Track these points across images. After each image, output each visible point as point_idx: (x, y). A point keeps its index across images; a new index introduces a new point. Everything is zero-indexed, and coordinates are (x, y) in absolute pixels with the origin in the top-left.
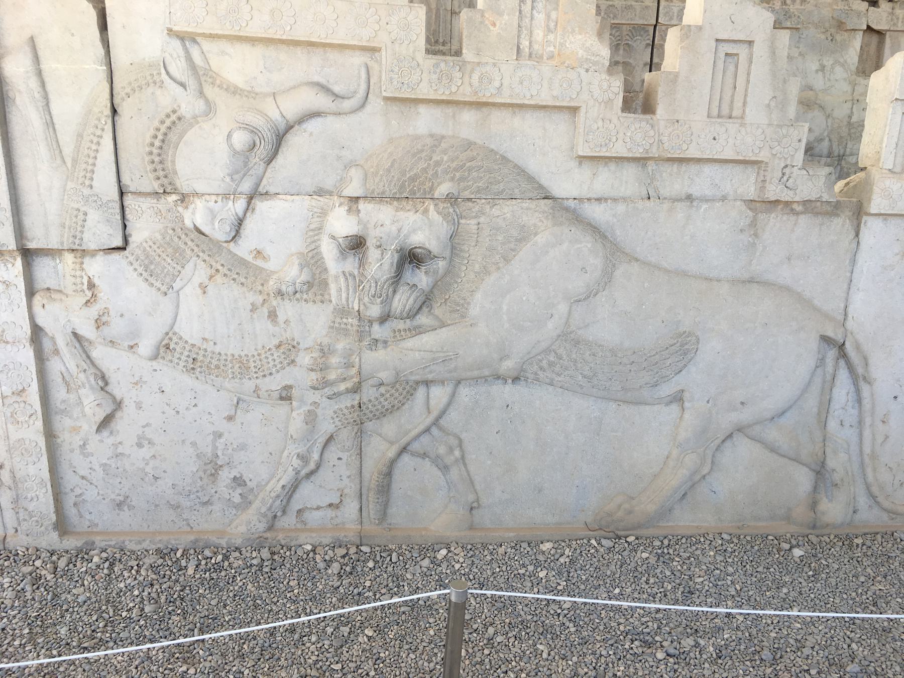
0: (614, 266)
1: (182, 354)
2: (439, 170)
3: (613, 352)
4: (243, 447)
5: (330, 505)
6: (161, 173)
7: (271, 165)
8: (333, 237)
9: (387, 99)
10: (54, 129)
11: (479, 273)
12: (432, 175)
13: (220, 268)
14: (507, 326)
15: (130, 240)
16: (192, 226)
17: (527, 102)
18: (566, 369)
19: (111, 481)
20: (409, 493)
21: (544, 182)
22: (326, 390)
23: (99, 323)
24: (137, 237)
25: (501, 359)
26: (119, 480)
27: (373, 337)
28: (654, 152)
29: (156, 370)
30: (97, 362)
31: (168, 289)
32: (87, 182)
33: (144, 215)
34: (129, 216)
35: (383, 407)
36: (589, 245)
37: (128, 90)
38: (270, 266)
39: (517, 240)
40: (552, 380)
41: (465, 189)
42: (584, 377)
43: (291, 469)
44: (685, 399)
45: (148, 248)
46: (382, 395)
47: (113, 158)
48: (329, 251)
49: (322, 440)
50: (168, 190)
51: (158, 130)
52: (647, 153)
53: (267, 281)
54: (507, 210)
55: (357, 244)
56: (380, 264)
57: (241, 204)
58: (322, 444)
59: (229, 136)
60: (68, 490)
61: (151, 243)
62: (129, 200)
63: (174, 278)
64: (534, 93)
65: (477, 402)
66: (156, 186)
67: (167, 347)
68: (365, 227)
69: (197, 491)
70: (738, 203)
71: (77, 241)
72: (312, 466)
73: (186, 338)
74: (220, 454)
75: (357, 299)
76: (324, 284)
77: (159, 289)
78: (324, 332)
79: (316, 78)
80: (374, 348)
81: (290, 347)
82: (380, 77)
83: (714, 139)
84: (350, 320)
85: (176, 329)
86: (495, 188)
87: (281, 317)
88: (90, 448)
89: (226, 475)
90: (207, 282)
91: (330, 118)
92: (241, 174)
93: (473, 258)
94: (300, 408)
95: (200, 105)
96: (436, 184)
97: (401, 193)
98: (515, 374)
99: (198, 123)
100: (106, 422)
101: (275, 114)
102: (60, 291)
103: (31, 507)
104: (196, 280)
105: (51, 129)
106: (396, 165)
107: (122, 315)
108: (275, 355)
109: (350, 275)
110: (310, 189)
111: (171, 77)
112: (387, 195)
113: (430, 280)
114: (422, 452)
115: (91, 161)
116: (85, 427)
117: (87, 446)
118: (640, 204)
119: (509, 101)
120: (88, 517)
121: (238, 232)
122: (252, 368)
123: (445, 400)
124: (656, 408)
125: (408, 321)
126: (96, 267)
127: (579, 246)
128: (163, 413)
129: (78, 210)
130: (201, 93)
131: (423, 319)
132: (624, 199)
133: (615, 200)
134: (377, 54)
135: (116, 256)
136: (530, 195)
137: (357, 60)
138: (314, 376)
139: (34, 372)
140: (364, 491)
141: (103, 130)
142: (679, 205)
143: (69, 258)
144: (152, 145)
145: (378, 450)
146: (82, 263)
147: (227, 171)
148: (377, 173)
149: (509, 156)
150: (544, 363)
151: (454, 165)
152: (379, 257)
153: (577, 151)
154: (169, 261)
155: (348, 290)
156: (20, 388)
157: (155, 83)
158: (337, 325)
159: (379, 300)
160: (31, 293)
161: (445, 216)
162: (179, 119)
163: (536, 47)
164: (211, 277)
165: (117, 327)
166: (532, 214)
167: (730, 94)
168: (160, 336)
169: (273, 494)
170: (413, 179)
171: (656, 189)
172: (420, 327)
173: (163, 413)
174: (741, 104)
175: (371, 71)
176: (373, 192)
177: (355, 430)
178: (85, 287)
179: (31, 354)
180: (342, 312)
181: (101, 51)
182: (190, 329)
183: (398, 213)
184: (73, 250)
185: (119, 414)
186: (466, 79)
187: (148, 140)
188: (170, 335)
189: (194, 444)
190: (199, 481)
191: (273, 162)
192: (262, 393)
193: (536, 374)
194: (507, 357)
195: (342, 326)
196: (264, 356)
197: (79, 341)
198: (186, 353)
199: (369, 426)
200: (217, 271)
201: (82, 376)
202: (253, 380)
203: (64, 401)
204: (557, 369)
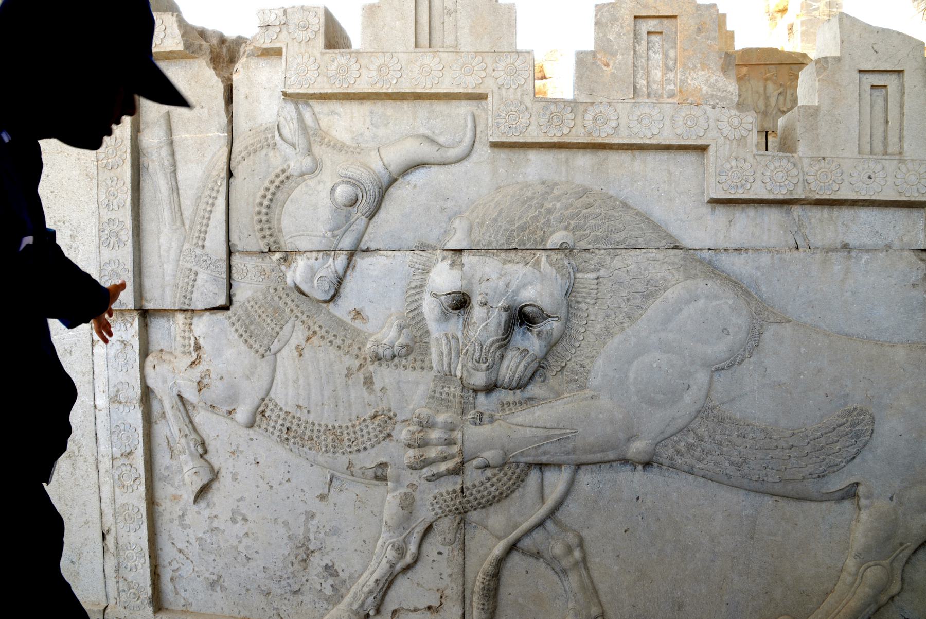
0: (761, 326)
1: (276, 422)
2: (552, 217)
3: (768, 434)
4: (335, 531)
5: (429, 608)
6: (268, 233)
7: (374, 220)
8: (435, 295)
9: (495, 145)
11: (600, 335)
12: (544, 223)
13: (317, 329)
14: (634, 398)
15: (234, 299)
16: (292, 285)
17: (647, 142)
18: (709, 453)
19: (206, 557)
20: (520, 600)
21: (674, 230)
22: (424, 470)
23: (201, 386)
24: (242, 294)
25: (629, 440)
26: (213, 557)
27: (478, 409)
28: (799, 194)
29: (252, 439)
30: (199, 428)
31: (266, 351)
32: (200, 243)
33: (249, 275)
34: (235, 275)
35: (489, 493)
36: (730, 302)
37: (244, 154)
38: (369, 327)
40: (692, 467)
41: (581, 239)
42: (732, 464)
43: (385, 560)
44: (860, 494)
46: (489, 479)
47: (224, 218)
49: (420, 530)
50: (273, 249)
51: (267, 189)
52: (791, 194)
53: (364, 344)
54: (631, 260)
55: (461, 303)
57: (341, 260)
58: (420, 534)
59: (333, 190)
60: (166, 563)
61: (252, 303)
62: (236, 259)
63: (273, 338)
64: (656, 131)
65: (600, 492)
67: (263, 412)
68: (470, 283)
69: (288, 578)
70: (906, 253)
72: (408, 559)
73: (281, 404)
74: (312, 537)
77: (257, 351)
79: (422, 131)
81: (386, 418)
83: (870, 177)
84: (452, 389)
85: (272, 394)
86: (616, 237)
87: (377, 386)
88: (187, 521)
89: (317, 562)
91: (435, 169)
92: (342, 230)
93: (592, 318)
94: (395, 490)
95: (307, 162)
97: (510, 244)
99: (305, 180)
100: (203, 492)
101: (377, 165)
102: (171, 353)
103: (130, 576)
104: (294, 342)
105: (175, 194)
106: (504, 214)
107: (221, 378)
108: (371, 427)
109: (453, 337)
110: (413, 244)
111: (283, 139)
112: (494, 245)
113: (543, 343)
114: (535, 551)
115: (205, 222)
116: (185, 496)
117: (186, 517)
118: (788, 256)
119: (627, 141)
120: (183, 594)
122: (346, 441)
124: (824, 505)
125: (518, 391)
126: (202, 326)
127: (718, 302)
128: (257, 486)
129: (190, 270)
130: (309, 151)
131: (534, 390)
132: (769, 249)
133: (757, 250)
134: (484, 102)
135: (220, 315)
136: (657, 245)
137: (463, 109)
138: (411, 452)
139: (141, 435)
140: (467, 593)
141: (218, 191)
142: (834, 256)
143: (180, 317)
144: (261, 204)
146: (191, 324)
147: (328, 227)
149: (630, 202)
151: (568, 212)
152: (485, 315)
153: (708, 194)
155: (450, 353)
156: (128, 450)
159: (484, 366)
160: (145, 353)
161: (560, 269)
162: (288, 178)
163: (655, 86)
164: (308, 339)
165: (217, 389)
167: (881, 130)
168: (257, 401)
169: (366, 589)
170: (523, 229)
171: (805, 237)
172: (531, 399)
173: (257, 486)
174: (896, 139)
175: (477, 120)
177: (458, 521)
178: (192, 348)
179: (139, 415)
181: (224, 119)
182: (285, 396)
183: (506, 266)
184: (184, 310)
185: (216, 485)
186: (579, 120)
187: (258, 200)
188: (266, 401)
189: (286, 524)
190: (290, 565)
191: (376, 217)
192: (355, 470)
193: (672, 459)
195: (444, 396)
196: (358, 428)
197: (184, 405)
198: (281, 422)
199: (474, 516)
200: (315, 333)
201: (183, 441)
202: (346, 455)
203: (167, 467)
204: (698, 453)
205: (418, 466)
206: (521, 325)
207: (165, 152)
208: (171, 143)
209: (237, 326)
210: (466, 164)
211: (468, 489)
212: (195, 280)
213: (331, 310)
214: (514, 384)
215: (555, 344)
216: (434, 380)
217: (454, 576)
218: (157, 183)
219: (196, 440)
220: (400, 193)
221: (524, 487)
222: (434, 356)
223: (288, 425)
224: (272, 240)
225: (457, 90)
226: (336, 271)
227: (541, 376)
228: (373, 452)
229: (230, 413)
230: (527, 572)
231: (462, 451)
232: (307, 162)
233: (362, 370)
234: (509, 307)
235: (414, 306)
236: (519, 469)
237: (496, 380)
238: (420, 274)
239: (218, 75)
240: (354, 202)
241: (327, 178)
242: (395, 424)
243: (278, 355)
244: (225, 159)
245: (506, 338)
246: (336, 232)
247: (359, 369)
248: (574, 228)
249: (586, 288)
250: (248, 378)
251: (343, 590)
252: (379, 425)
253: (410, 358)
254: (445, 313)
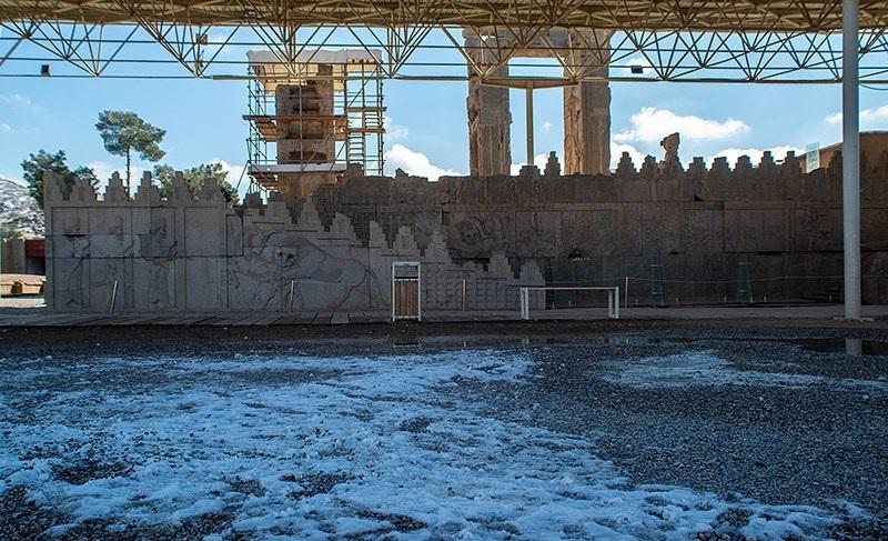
55: (281, 254)
56: (285, 257)
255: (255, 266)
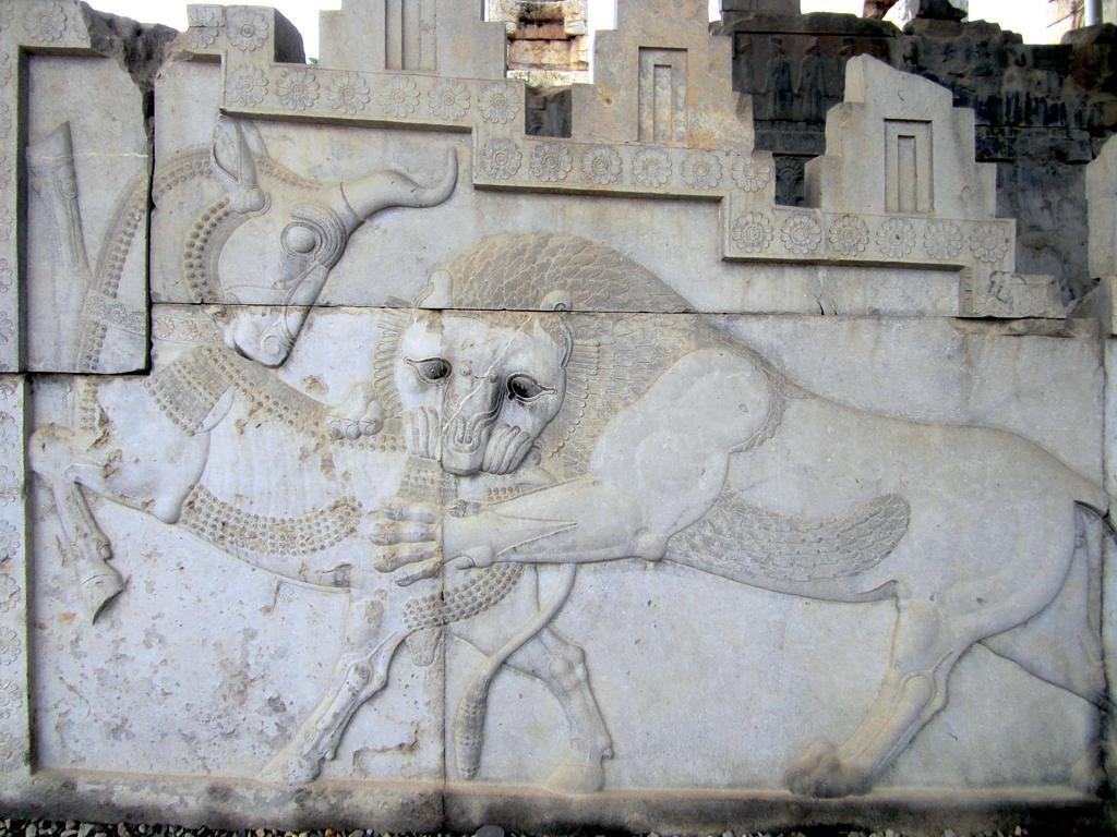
1: (208, 516)
2: (546, 276)
4: (281, 654)
9: (478, 188)
10: (80, 226)
16: (232, 346)
17: (654, 191)
23: (108, 471)
24: (165, 357)
25: (637, 533)
27: (460, 498)
31: (197, 426)
32: (111, 290)
34: (156, 331)
35: (475, 599)
36: (748, 374)
37: (170, 181)
39: (651, 367)
41: (580, 299)
42: (755, 560)
45: (176, 373)
46: (474, 582)
48: (404, 378)
49: (391, 646)
50: (206, 301)
51: (200, 227)
54: (631, 329)
55: (441, 371)
56: (470, 396)
57: (294, 318)
58: (390, 653)
59: (285, 233)
61: (180, 367)
62: (158, 313)
64: (663, 180)
66: (193, 295)
68: (451, 349)
71: (91, 363)
72: (375, 685)
73: (215, 493)
74: (251, 661)
75: (439, 444)
76: (397, 427)
77: (186, 427)
78: (395, 490)
79: (393, 166)
80: (461, 513)
81: (349, 510)
82: (472, 163)
84: (430, 474)
85: (203, 481)
87: (339, 469)
89: (259, 695)
90: (245, 418)
96: (542, 293)
97: (497, 304)
98: (658, 554)
99: (248, 218)
101: (339, 206)
104: (233, 416)
105: (77, 228)
107: (137, 461)
121: (289, 354)
123: (561, 592)
125: (508, 476)
127: (734, 375)
128: (181, 599)
129: (97, 324)
130: (254, 184)
131: (528, 474)
134: (467, 137)
135: (137, 382)
136: (666, 308)
138: (380, 551)
141: (136, 227)
144: (192, 245)
145: (469, 664)
146: (96, 392)
147: (278, 277)
148: (466, 277)
150: (697, 540)
151: (565, 268)
152: (468, 387)
154: (201, 389)
155: (428, 431)
157: (202, 173)
158: (412, 481)
159: (467, 446)
160: (30, 429)
161: (555, 334)
162: (227, 214)
163: (662, 127)
166: (670, 334)
169: (321, 726)
170: (512, 286)
176: (460, 302)
179: (21, 509)
180: (421, 460)
181: (144, 138)
182: (220, 483)
184: (87, 375)
185: (124, 598)
187: (188, 239)
194: (646, 529)
197: (83, 495)
199: (454, 626)
200: (260, 404)
201: (81, 542)
203: (56, 577)
205: (388, 568)
206: (511, 397)
207: (63, 173)
208: (71, 162)
209: (159, 395)
210: (446, 207)
211: (449, 594)
212: (103, 337)
213: (280, 378)
214: (503, 468)
215: (550, 421)
216: (408, 463)
217: (432, 705)
218: (50, 214)
219: (99, 541)
220: (366, 238)
221: (515, 591)
222: (409, 434)
223: (224, 520)
224: (206, 289)
225: (435, 122)
226: (288, 331)
227: (536, 458)
228: (333, 551)
229: (147, 504)
230: (521, 696)
231: (442, 549)
232: (251, 198)
233: (320, 451)
234: (497, 377)
235: (384, 373)
236: (508, 568)
237: (482, 464)
238: (392, 336)
239: (135, 80)
240: (310, 249)
241: (278, 217)
242: (360, 516)
243: (212, 432)
244: (146, 188)
245: (493, 413)
246: (289, 283)
247: (316, 450)
248: (570, 287)
249: (586, 356)
250: (172, 460)
251: (291, 730)
252: (341, 518)
253: (379, 435)
254: (421, 384)
255: (244, 457)
